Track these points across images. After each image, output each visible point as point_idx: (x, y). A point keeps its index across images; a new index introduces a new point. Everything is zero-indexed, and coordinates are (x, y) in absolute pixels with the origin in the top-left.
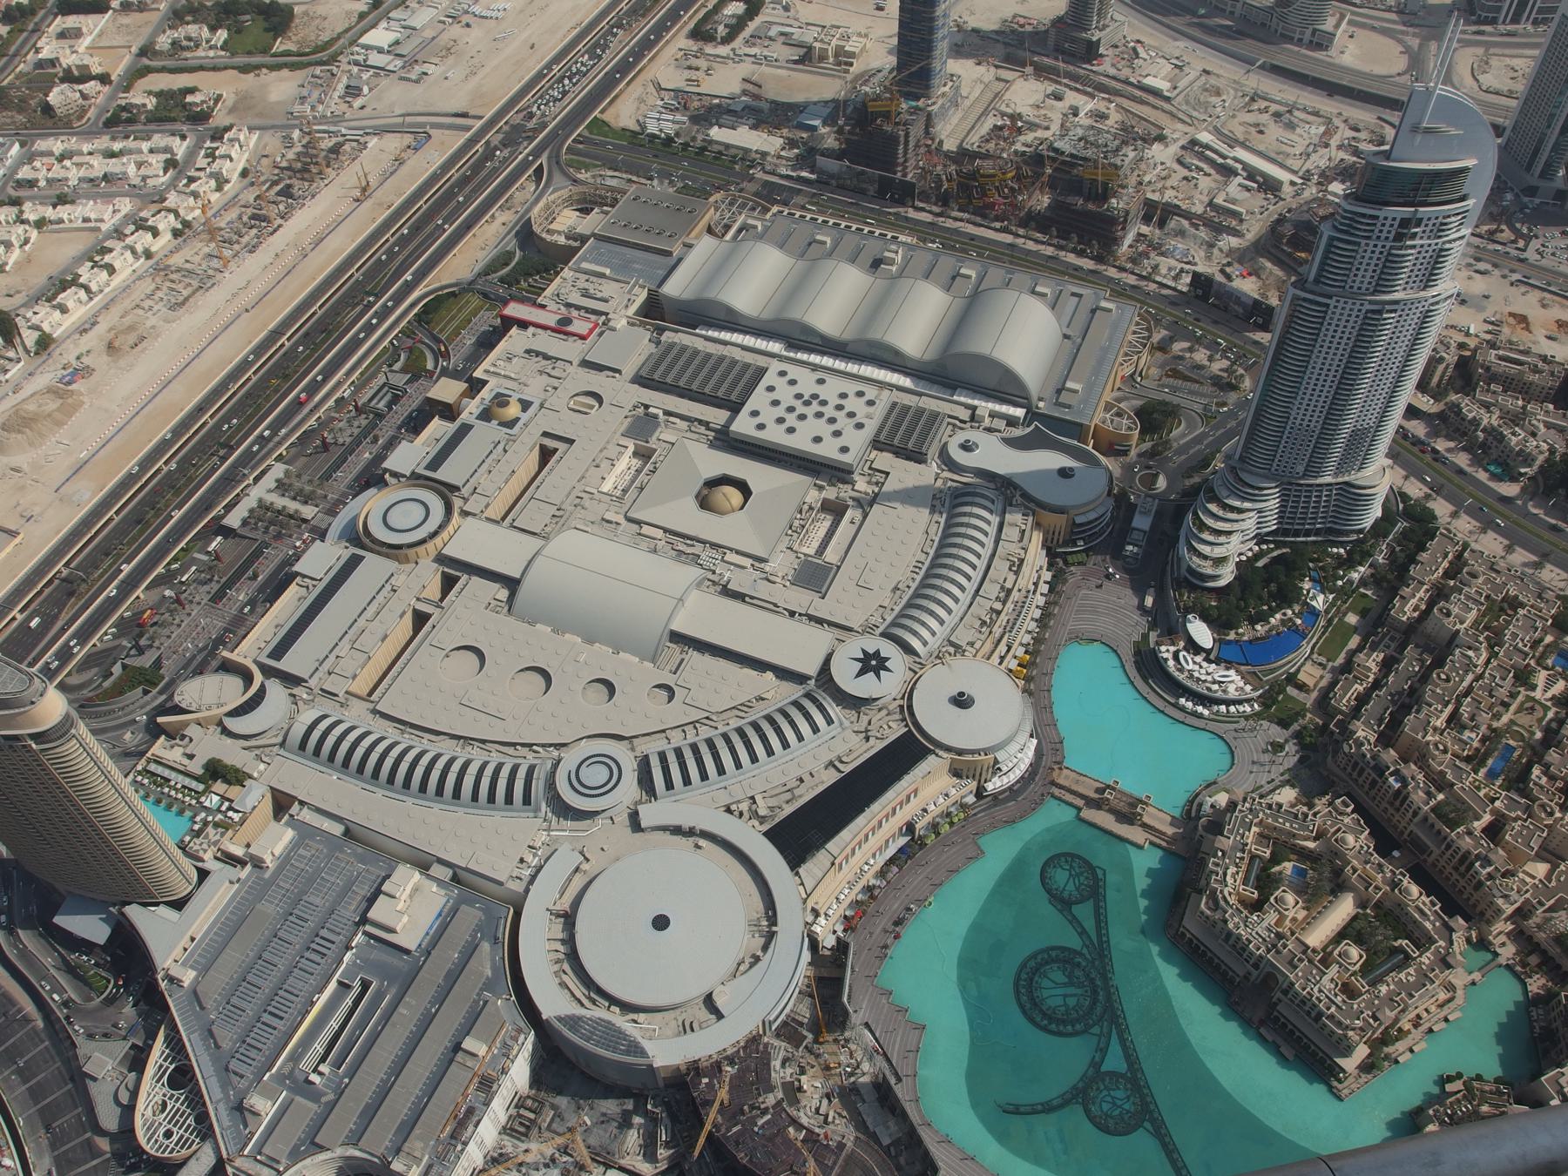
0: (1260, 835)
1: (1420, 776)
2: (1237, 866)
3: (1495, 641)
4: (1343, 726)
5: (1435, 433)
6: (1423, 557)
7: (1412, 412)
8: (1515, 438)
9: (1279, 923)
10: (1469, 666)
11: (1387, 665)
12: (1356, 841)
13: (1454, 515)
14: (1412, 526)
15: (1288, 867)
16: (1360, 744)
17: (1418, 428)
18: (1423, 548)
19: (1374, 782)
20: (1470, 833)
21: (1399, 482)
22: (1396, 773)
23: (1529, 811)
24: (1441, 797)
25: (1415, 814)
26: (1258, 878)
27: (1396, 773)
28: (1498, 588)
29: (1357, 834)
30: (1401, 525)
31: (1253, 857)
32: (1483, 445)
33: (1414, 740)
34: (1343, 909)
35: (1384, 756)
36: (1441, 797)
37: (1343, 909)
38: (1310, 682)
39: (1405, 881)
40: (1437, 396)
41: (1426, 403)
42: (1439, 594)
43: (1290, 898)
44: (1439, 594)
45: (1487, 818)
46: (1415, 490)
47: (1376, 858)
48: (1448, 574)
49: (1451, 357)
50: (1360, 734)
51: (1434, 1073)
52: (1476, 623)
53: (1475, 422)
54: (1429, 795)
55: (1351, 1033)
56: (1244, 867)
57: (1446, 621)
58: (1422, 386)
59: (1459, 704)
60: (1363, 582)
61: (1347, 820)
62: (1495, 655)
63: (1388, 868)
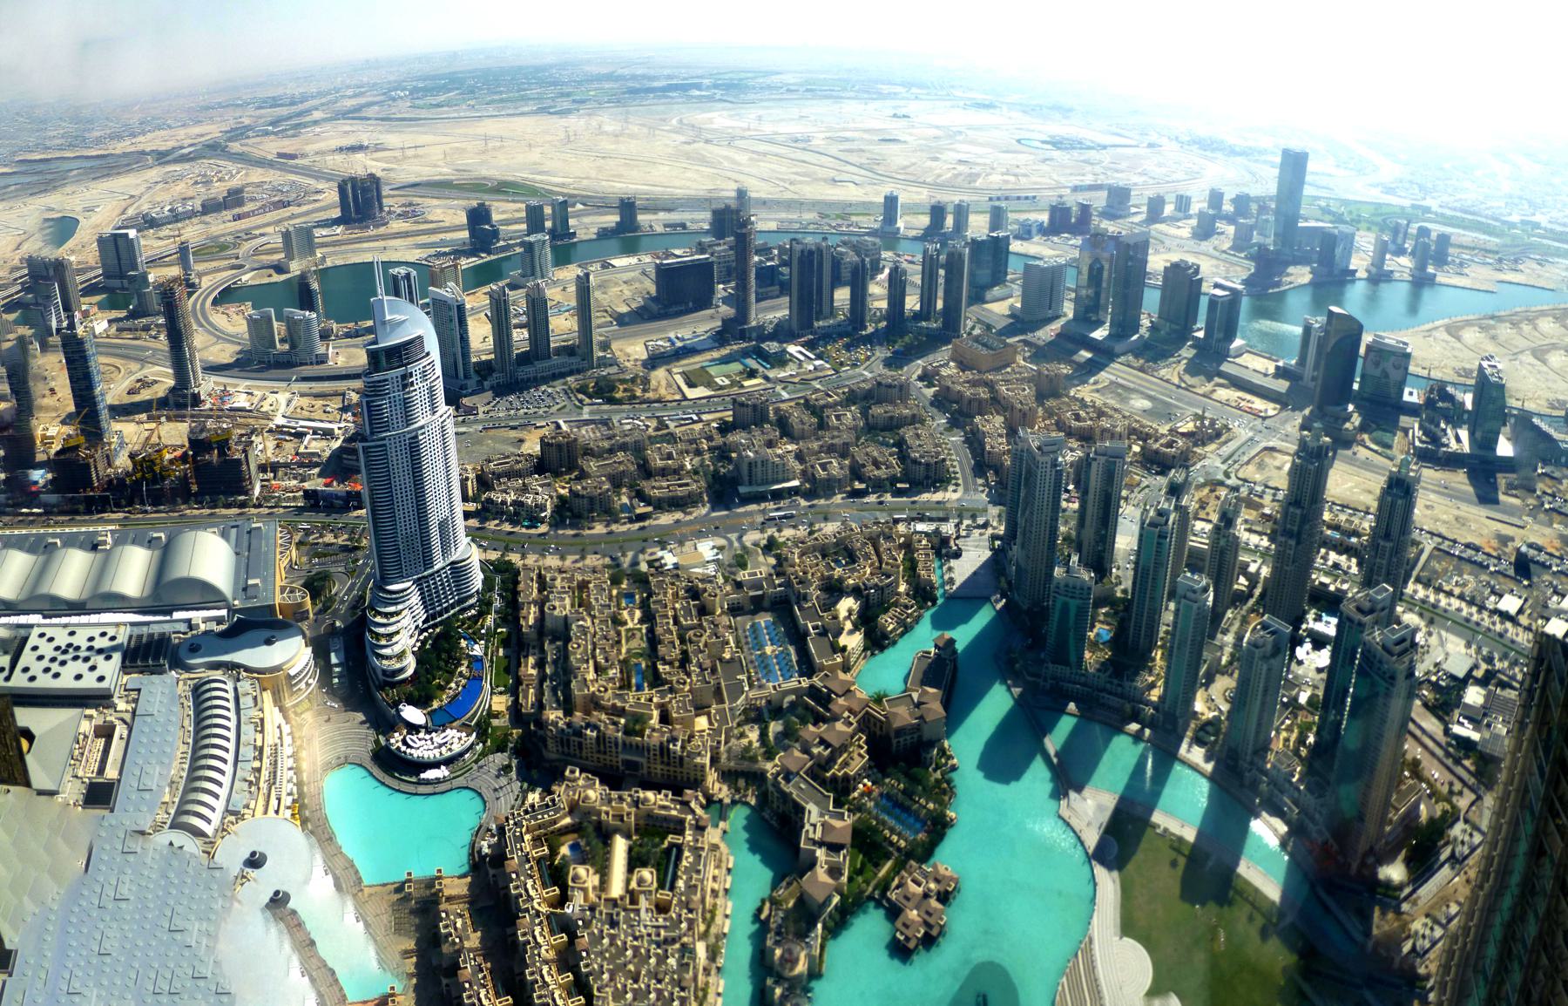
0: (534, 839)
1: (604, 717)
2: (531, 877)
3: (589, 608)
4: (541, 724)
5: (483, 520)
6: (521, 587)
7: (467, 515)
8: (529, 500)
9: (586, 899)
10: (584, 630)
11: (540, 665)
12: (595, 793)
13: (523, 557)
14: (504, 576)
15: (565, 850)
16: (555, 724)
17: (474, 522)
18: (518, 583)
19: (580, 744)
20: (654, 730)
21: (483, 557)
22: (588, 725)
23: (671, 690)
24: (623, 721)
25: (616, 744)
26: (551, 876)
27: (588, 725)
28: (571, 580)
29: (592, 786)
30: (498, 579)
31: (539, 861)
32: (516, 513)
33: (585, 697)
34: (620, 846)
35: (575, 720)
36: (623, 721)
37: (620, 846)
38: (502, 708)
39: (641, 795)
40: (474, 500)
41: (472, 507)
42: (541, 604)
43: (581, 870)
44: (541, 604)
45: (656, 713)
46: (494, 556)
47: (614, 794)
48: (540, 591)
49: (472, 476)
50: (552, 717)
51: (748, 917)
52: (573, 605)
53: (504, 502)
54: (615, 724)
55: (685, 939)
56: (537, 876)
57: (556, 613)
58: (465, 499)
59: (594, 657)
60: (497, 626)
61: (581, 782)
62: (593, 617)
63: (625, 794)
